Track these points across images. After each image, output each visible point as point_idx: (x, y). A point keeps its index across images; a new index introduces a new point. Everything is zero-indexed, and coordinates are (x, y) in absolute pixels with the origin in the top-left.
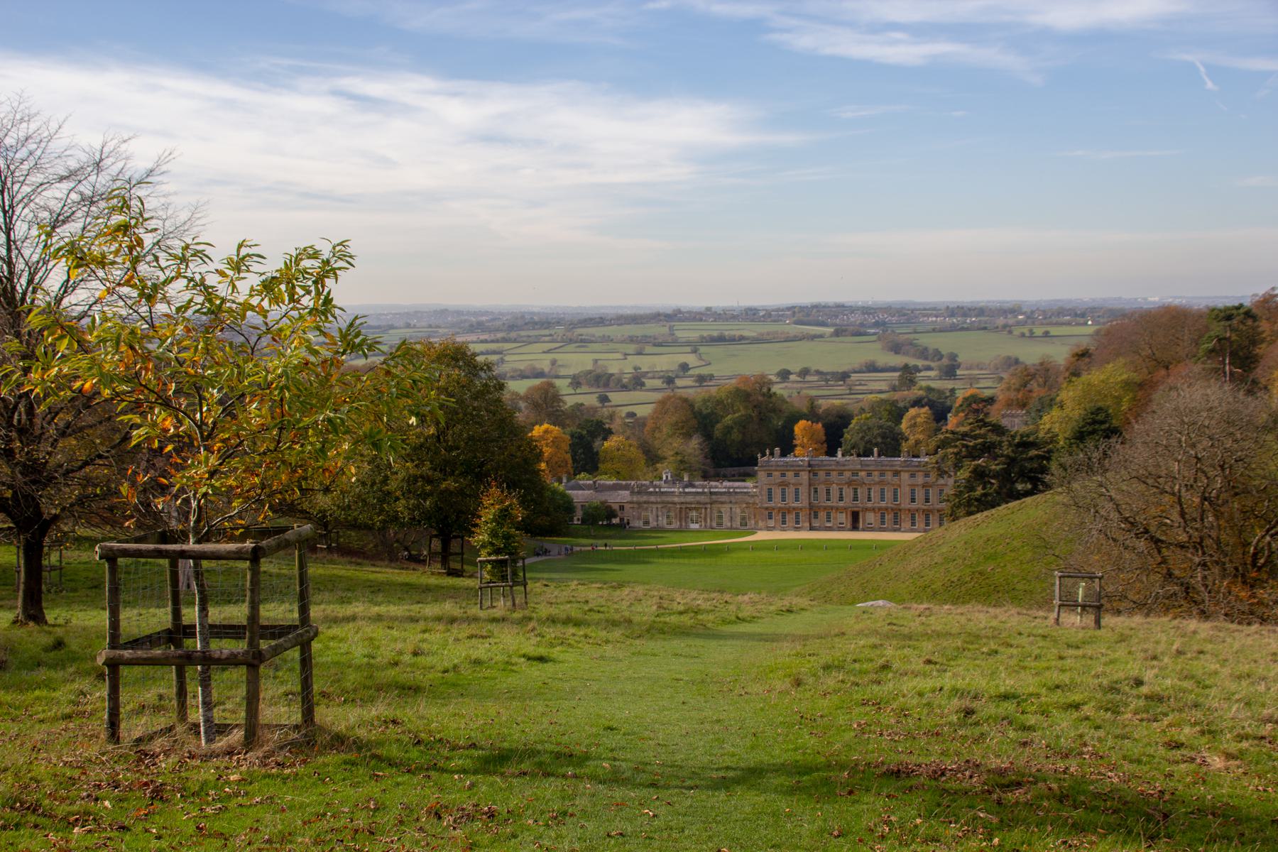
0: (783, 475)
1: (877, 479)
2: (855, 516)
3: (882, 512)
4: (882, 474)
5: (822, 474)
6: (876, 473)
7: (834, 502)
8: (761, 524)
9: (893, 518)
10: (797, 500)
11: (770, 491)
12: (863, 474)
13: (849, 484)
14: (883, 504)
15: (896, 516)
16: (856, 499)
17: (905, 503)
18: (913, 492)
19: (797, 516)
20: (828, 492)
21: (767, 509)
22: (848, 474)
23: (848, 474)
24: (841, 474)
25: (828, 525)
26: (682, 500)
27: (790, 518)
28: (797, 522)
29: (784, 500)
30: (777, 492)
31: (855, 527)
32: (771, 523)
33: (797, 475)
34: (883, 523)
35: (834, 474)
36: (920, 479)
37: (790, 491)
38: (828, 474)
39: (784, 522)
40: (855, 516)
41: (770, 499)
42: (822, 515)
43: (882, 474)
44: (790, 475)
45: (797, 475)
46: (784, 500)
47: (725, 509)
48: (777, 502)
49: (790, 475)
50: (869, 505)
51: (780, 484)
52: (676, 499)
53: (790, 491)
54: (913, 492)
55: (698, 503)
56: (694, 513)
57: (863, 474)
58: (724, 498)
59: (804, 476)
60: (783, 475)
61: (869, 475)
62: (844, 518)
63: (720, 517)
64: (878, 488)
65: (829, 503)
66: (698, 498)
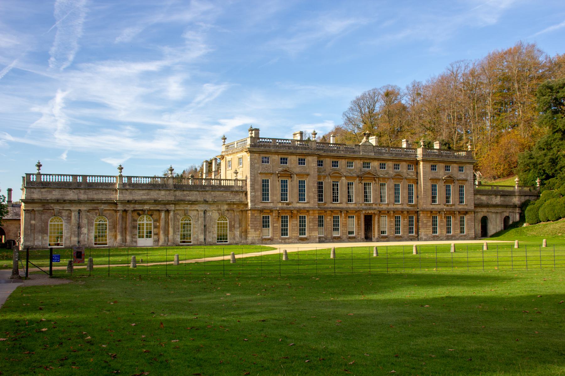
0: (284, 161)
1: (392, 172)
2: (368, 220)
3: (396, 215)
4: (396, 167)
5: (328, 162)
6: (390, 164)
7: (342, 204)
8: (252, 235)
9: (410, 221)
10: (301, 198)
11: (265, 184)
12: (375, 164)
13: (360, 178)
14: (398, 206)
15: (411, 222)
16: (366, 198)
17: (425, 203)
18: (434, 188)
20: (335, 186)
21: (261, 211)
22: (357, 164)
24: (349, 164)
25: (335, 234)
26: (128, 197)
27: (293, 225)
29: (284, 197)
30: (275, 186)
31: (368, 238)
32: (269, 233)
33: (301, 162)
34: (397, 231)
35: (342, 163)
36: (441, 172)
37: (292, 185)
38: (335, 164)
39: (284, 232)
40: (368, 220)
41: (265, 197)
42: (328, 220)
43: (396, 167)
44: (293, 160)
45: (301, 162)
46: (284, 197)
47: (195, 212)
48: (274, 201)
49: (293, 160)
50: (384, 207)
51: (280, 175)
52: (117, 196)
53: (292, 185)
54: (434, 188)
55: (156, 202)
56: (145, 221)
57: (375, 164)
58: (194, 196)
59: (311, 162)
60: (284, 161)
61: (382, 166)
62: (354, 225)
63: (186, 226)
64: (392, 183)
65: (336, 205)
66: (154, 195)
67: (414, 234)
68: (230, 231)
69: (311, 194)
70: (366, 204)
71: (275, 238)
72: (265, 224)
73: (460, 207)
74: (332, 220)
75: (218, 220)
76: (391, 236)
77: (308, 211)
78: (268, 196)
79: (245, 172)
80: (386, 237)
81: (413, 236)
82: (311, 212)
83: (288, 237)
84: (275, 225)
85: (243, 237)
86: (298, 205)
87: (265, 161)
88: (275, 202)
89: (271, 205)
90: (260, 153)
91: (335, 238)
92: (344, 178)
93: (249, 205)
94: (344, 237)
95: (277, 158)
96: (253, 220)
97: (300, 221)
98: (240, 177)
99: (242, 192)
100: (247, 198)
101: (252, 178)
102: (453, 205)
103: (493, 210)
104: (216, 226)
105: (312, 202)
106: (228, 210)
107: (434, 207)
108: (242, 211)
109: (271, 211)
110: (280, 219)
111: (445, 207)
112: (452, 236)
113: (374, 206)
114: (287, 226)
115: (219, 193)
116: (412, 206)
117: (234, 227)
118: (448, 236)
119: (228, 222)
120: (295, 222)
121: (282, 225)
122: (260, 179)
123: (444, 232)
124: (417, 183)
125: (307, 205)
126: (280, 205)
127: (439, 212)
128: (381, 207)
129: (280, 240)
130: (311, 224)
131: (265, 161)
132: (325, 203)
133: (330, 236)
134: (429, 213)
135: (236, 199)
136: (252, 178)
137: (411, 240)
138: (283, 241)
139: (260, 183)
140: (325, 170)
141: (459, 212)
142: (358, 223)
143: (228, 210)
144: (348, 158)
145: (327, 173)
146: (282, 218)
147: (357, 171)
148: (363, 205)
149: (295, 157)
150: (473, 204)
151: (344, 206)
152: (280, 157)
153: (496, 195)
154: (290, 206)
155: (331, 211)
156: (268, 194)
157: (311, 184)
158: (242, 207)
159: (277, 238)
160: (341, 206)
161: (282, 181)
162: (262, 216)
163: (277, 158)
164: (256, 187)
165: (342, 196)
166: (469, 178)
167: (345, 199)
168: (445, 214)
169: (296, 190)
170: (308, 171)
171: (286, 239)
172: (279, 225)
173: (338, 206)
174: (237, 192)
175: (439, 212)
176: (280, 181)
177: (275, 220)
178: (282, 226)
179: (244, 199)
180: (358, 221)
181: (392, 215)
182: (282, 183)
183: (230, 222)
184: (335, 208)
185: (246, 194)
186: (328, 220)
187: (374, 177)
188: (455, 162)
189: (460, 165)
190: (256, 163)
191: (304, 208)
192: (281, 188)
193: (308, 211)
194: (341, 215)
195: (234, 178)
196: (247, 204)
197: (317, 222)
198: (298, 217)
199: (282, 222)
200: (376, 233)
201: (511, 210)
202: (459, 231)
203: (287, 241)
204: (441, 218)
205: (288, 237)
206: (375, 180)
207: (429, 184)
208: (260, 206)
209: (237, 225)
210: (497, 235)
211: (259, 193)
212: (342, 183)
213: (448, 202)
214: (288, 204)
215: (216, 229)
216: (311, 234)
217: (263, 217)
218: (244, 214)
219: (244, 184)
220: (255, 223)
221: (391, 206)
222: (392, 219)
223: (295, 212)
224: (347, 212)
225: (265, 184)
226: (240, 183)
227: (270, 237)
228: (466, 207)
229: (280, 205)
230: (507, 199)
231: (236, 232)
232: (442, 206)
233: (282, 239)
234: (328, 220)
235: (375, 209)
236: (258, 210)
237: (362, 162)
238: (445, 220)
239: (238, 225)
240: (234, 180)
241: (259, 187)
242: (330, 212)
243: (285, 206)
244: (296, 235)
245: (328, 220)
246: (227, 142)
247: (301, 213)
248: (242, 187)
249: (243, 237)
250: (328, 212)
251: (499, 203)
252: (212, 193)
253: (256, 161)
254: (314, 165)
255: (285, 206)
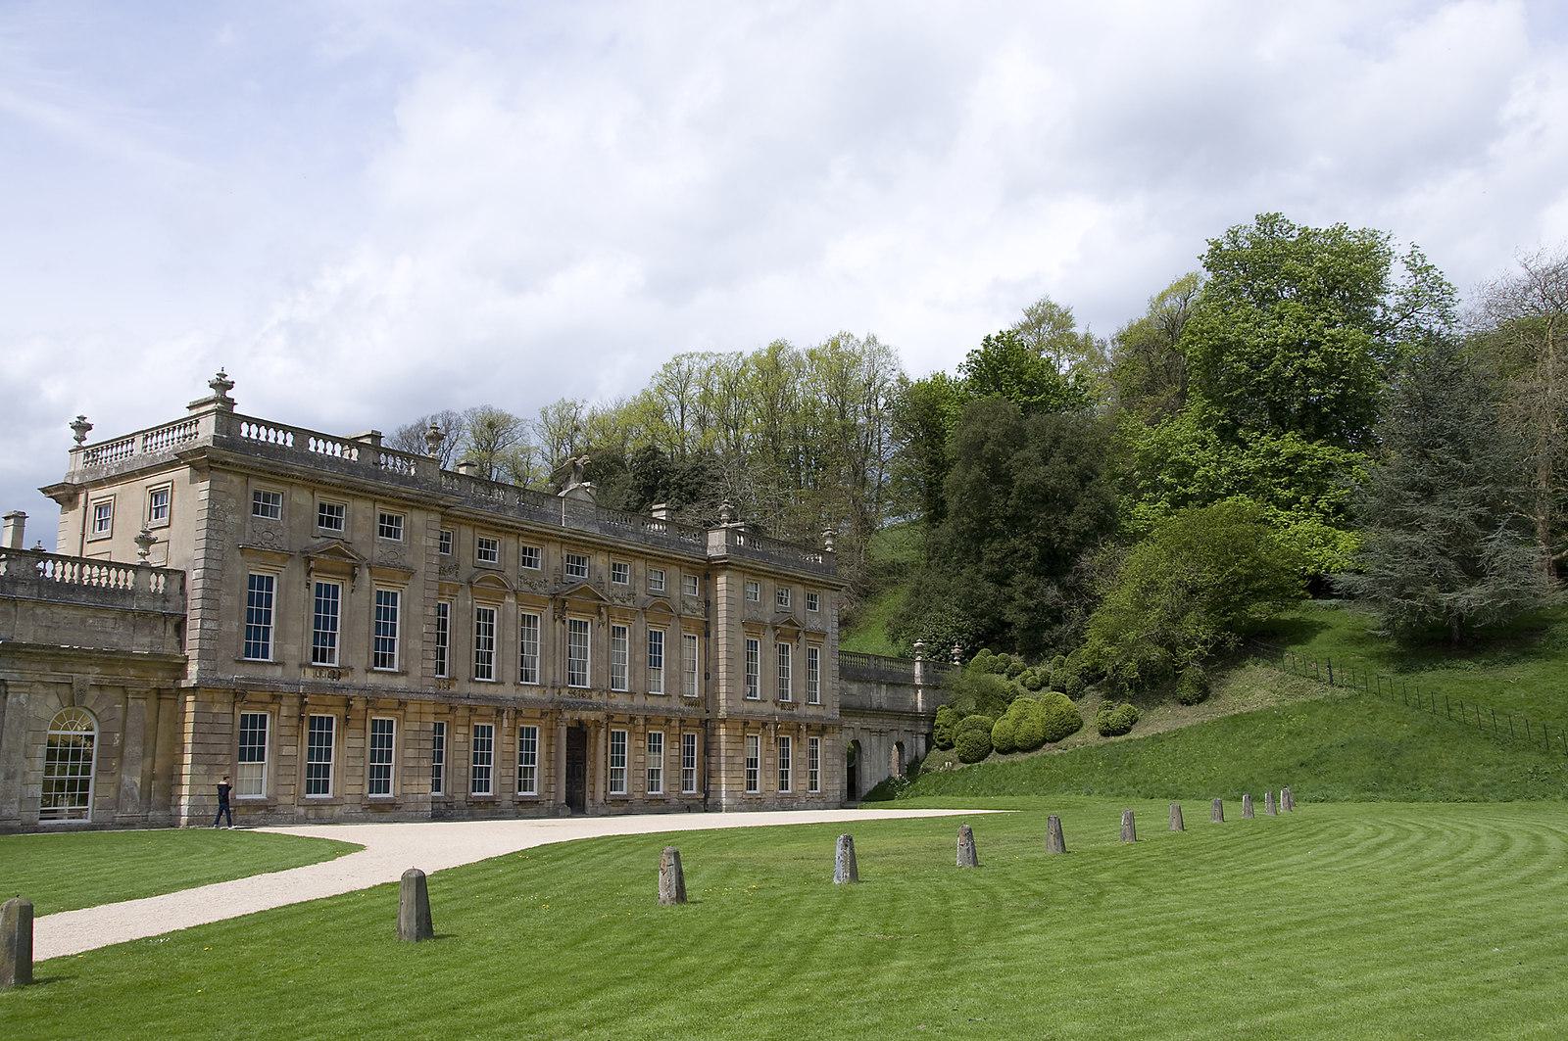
0: (329, 517)
11: (259, 592)
13: (560, 604)
19: (381, 736)
21: (238, 694)
22: (551, 558)
23: (551, 558)
27: (347, 752)
28: (379, 779)
31: (576, 806)
33: (388, 527)
35: (508, 550)
37: (354, 605)
38: (485, 550)
39: (317, 778)
41: (255, 642)
44: (360, 518)
45: (388, 527)
49: (360, 518)
50: (621, 701)
57: (600, 562)
60: (329, 517)
61: (617, 571)
67: (694, 791)
68: (99, 770)
69: (416, 645)
70: (572, 691)
71: (283, 800)
72: (250, 747)
73: (811, 711)
74: (472, 738)
75: (55, 727)
76: (638, 796)
77: (402, 704)
78: (266, 638)
79: (184, 542)
80: (624, 800)
81: (691, 797)
82: (411, 708)
83: (329, 796)
84: (286, 750)
85: (156, 798)
86: (372, 679)
87: (263, 505)
88: (293, 663)
89: (279, 671)
90: (248, 473)
91: (477, 802)
92: (510, 600)
93: (193, 669)
94: (508, 797)
95: (305, 501)
96: (204, 728)
97: (374, 737)
98: (155, 560)
99: (165, 617)
100: (182, 643)
101: (213, 565)
102: (795, 704)
103: (873, 723)
104: (42, 750)
105: (416, 672)
106: (101, 687)
107: (747, 706)
108: (159, 691)
109: (276, 698)
110: (306, 731)
111: (778, 710)
112: (793, 797)
113: (595, 698)
114: (328, 758)
115: (70, 613)
116: (691, 702)
117: (120, 753)
118: (784, 797)
119: (95, 733)
120: (359, 743)
121: (311, 751)
122: (242, 569)
123: (775, 787)
124: (707, 634)
125: (401, 683)
126: (309, 675)
127: (764, 724)
128: (614, 702)
129: (302, 811)
130: (410, 753)
131: (263, 505)
132: (453, 679)
133: (461, 797)
134: (741, 726)
135: (141, 644)
136: (213, 565)
137: (689, 809)
138: (311, 814)
139: (241, 588)
140: (457, 566)
141: (808, 726)
142: (549, 753)
143: (101, 687)
144: (529, 534)
145: (464, 577)
146: (312, 727)
147: (551, 579)
148: (565, 692)
149: (370, 504)
150: (837, 705)
151: (507, 691)
152: (321, 498)
153: (879, 683)
154: (343, 680)
155: (471, 709)
156: (267, 630)
157: (416, 609)
158: (157, 679)
159: (289, 800)
160: (500, 691)
161: (319, 585)
162: (239, 713)
163: (305, 501)
164: (227, 601)
165: (501, 662)
166: (829, 630)
167: (511, 673)
168: (776, 730)
169: (365, 627)
170: (408, 560)
171: (320, 804)
172: (298, 751)
173: (491, 690)
174: (144, 614)
175: (764, 724)
176: (313, 588)
177: (285, 731)
178: (311, 757)
179: (169, 647)
180: (549, 745)
181: (641, 729)
182: (318, 594)
183: (101, 733)
184: (487, 698)
185: (180, 627)
186: (459, 738)
187: (599, 606)
188: (801, 581)
189: (812, 591)
190: (232, 511)
191: (391, 691)
192: (313, 614)
193: (402, 704)
194: (499, 727)
195: (138, 561)
196: (181, 669)
197: (430, 745)
198: (369, 725)
199: (311, 742)
200: (598, 789)
201: (906, 725)
202: (807, 781)
203: (326, 811)
204: (768, 743)
205: (329, 796)
206: (600, 614)
207: (741, 639)
208: (238, 674)
209: (133, 749)
210: (882, 794)
211: (235, 626)
212: (504, 616)
213: (784, 695)
214: (336, 674)
215: (40, 764)
216: (407, 789)
217: (244, 717)
218: (166, 705)
219: (176, 586)
220: (213, 739)
221: (639, 701)
222: (641, 744)
223: (359, 705)
224: (518, 712)
225: (259, 592)
226: (157, 583)
227: (263, 796)
228: (821, 712)
229: (309, 675)
230: (901, 692)
231: (126, 779)
232: (769, 708)
233: (309, 805)
234: (459, 740)
235: (598, 708)
236: (227, 691)
237: (565, 553)
238: (775, 749)
239: (138, 749)
240: (136, 568)
241: (234, 600)
242: (467, 714)
243: (326, 680)
244: (357, 790)
245: (459, 738)
246: (92, 438)
247: (377, 710)
248: (165, 598)
249: (156, 798)
250: (459, 713)
251: (885, 706)
252: (39, 611)
253: (232, 503)
254: (431, 543)
255: (326, 680)
